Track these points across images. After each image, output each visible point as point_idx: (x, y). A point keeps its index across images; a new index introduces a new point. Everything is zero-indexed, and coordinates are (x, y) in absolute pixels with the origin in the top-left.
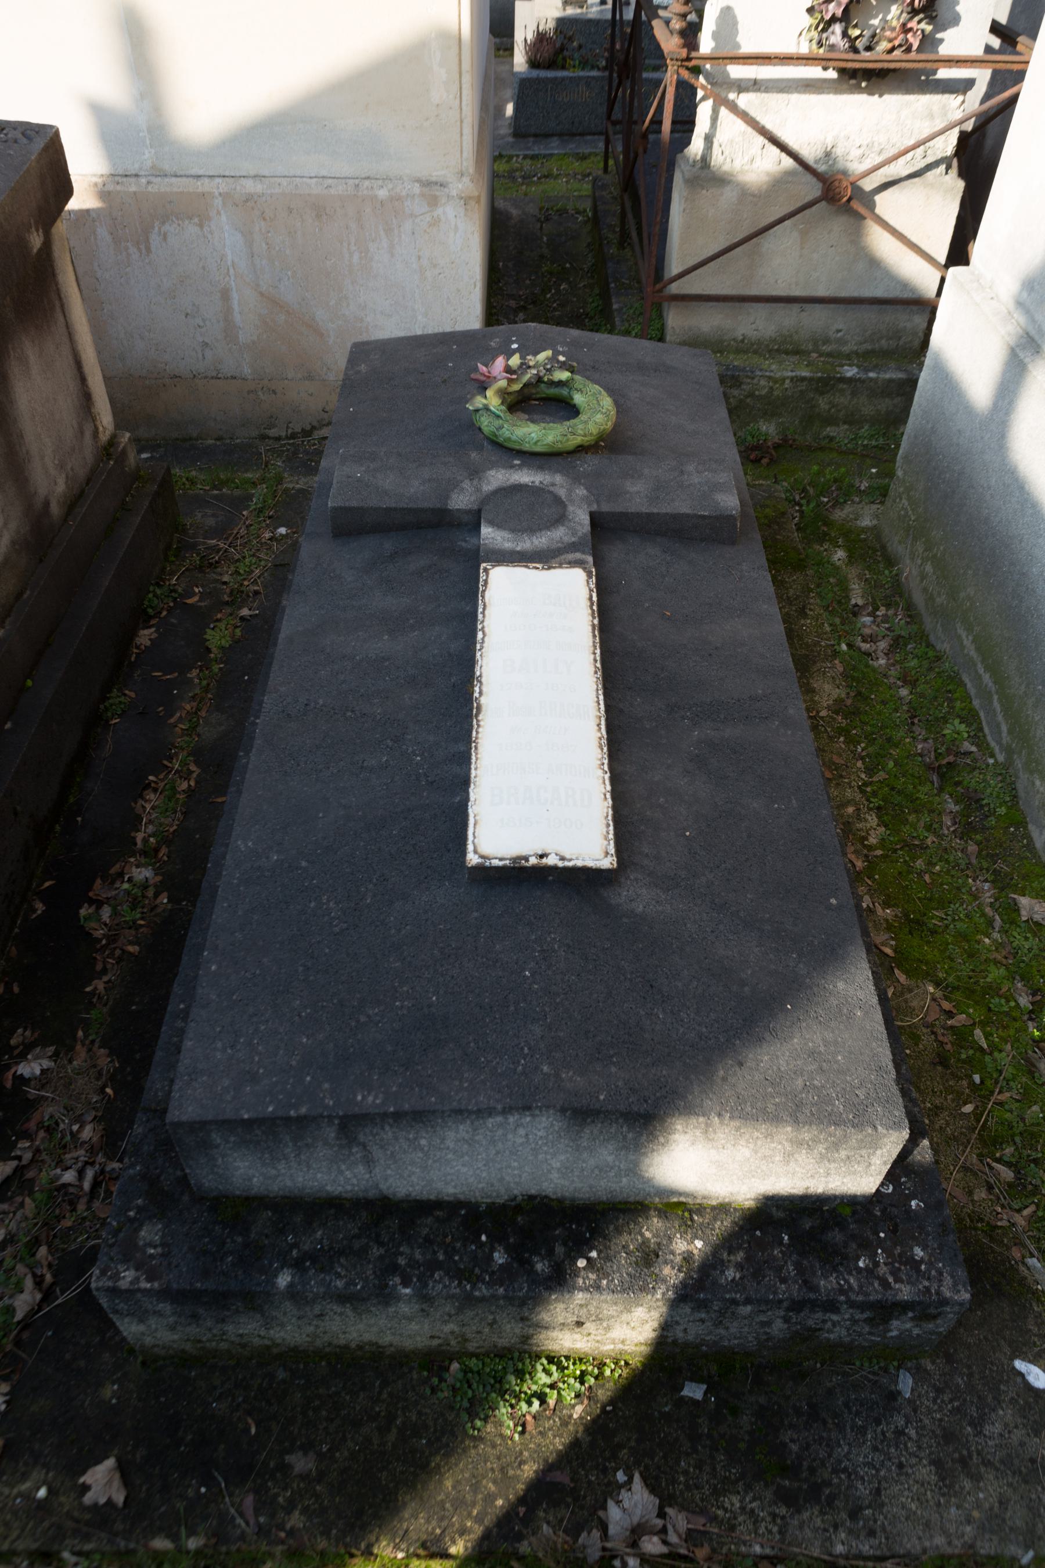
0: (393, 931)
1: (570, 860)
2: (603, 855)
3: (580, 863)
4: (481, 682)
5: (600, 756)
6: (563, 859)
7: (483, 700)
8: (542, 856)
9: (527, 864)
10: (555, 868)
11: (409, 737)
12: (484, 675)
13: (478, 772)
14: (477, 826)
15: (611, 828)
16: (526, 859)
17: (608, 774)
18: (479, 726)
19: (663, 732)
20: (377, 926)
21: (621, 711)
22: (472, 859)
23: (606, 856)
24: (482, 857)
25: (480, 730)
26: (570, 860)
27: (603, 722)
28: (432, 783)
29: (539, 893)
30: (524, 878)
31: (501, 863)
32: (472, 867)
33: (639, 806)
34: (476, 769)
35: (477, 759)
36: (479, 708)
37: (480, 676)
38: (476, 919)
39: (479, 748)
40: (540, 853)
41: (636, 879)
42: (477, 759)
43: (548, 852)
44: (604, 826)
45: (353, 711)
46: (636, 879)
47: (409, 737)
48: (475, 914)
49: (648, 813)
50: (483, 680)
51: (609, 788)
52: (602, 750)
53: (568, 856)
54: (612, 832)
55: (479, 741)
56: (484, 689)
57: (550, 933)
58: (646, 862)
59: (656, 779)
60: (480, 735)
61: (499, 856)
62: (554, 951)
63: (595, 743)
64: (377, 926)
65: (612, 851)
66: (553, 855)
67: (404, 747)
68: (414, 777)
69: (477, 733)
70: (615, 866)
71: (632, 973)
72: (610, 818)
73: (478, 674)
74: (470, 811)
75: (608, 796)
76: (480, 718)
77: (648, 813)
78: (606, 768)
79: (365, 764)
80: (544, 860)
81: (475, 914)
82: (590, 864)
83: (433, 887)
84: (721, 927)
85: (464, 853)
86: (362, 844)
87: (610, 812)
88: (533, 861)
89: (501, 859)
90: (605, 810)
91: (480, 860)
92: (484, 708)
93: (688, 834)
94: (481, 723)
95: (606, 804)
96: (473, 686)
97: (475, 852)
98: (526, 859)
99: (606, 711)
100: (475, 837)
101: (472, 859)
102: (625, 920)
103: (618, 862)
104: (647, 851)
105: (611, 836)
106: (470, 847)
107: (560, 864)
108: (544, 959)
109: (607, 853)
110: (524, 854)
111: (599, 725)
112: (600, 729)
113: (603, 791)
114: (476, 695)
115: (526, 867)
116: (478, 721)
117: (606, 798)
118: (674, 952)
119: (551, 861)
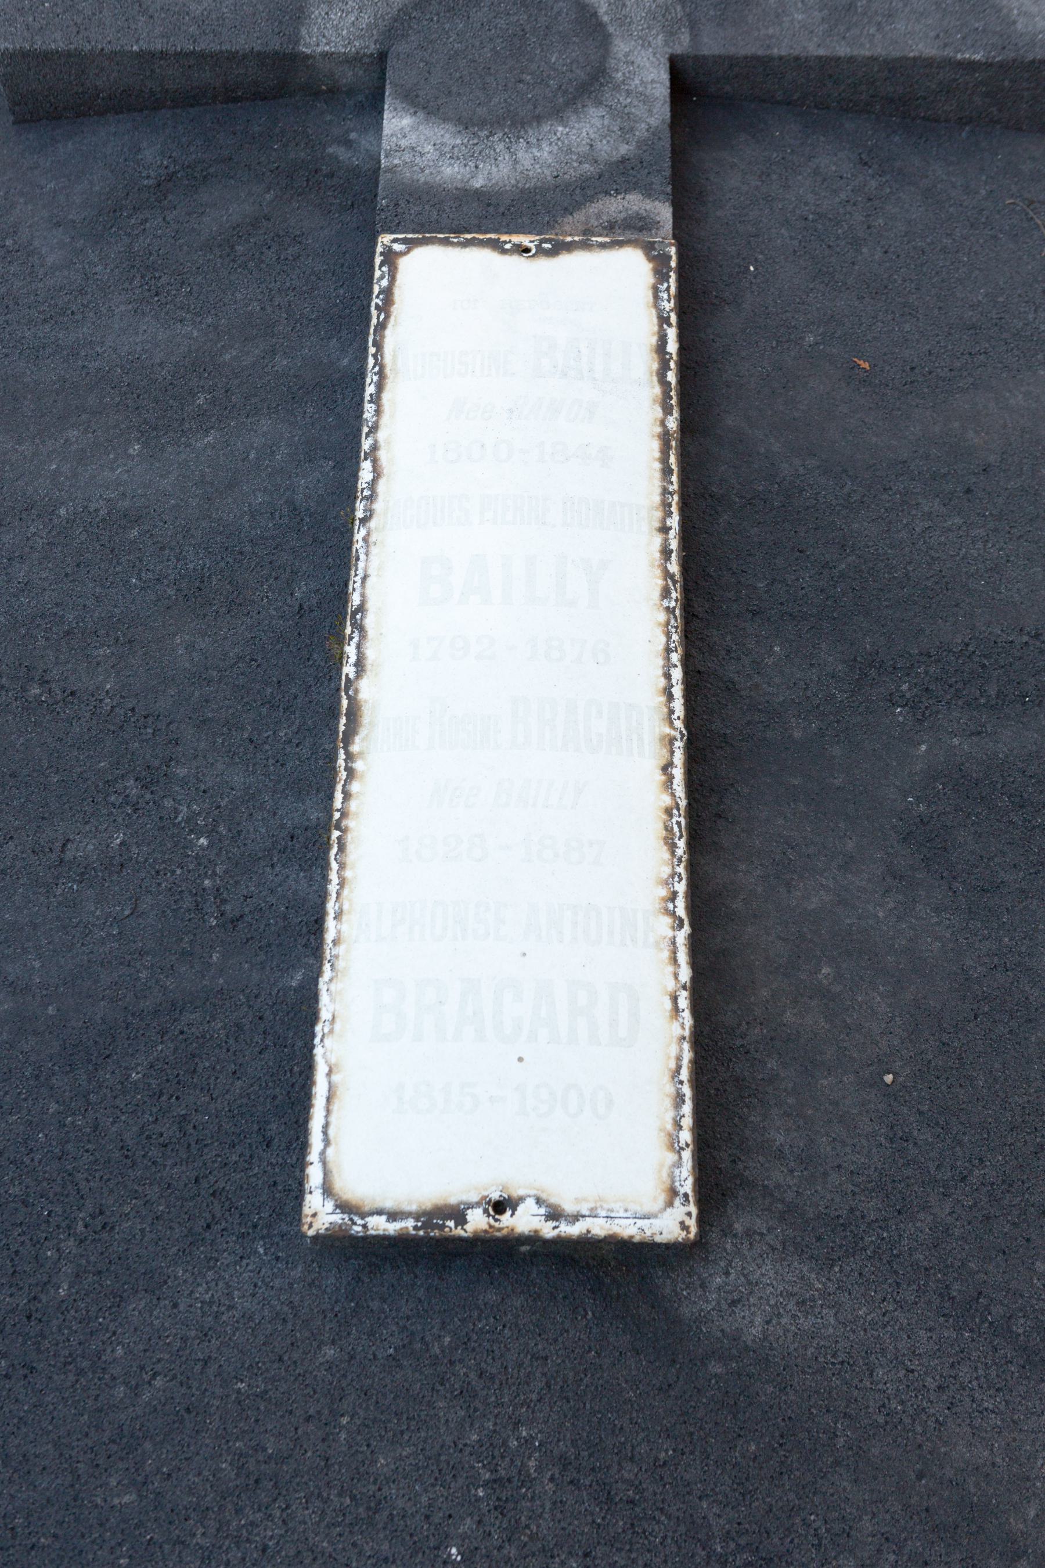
0: (120, 1391)
1: (576, 1218)
2: (662, 1198)
3: (599, 1228)
4: (360, 628)
5: (667, 871)
6: (554, 1215)
7: (367, 690)
8: (500, 1207)
9: (459, 1232)
10: (534, 1239)
11: (181, 772)
12: (370, 605)
13: (344, 927)
14: (335, 1107)
15: (687, 1108)
16: (459, 1215)
17: (687, 929)
18: (351, 772)
19: (837, 751)
20: (80, 1372)
21: (731, 688)
22: (319, 1213)
23: (670, 1204)
24: (344, 1207)
25: (355, 787)
26: (576, 1218)
27: (679, 758)
28: (235, 921)
29: (492, 1296)
30: (456, 1266)
31: (392, 1228)
32: (316, 1238)
33: (765, 993)
34: (338, 916)
35: (342, 884)
36: (354, 714)
37: (361, 609)
38: (330, 1366)
39: (350, 847)
40: (495, 1196)
41: (749, 1233)
42: (342, 884)
43: (517, 1192)
44: (668, 1103)
45: (44, 682)
46: (749, 1233)
47: (181, 772)
48: (330, 1352)
49: (789, 1016)
50: (370, 622)
51: (685, 974)
52: (672, 847)
53: (569, 1208)
54: (687, 1122)
55: (350, 823)
56: (370, 653)
57: (517, 1424)
58: (777, 1176)
59: (813, 904)
60: (353, 805)
61: (389, 1204)
62: (526, 1481)
63: (652, 827)
64: (80, 1372)
65: (687, 1187)
66: (530, 1202)
67: (168, 803)
68: (188, 903)
69: (347, 796)
70: (694, 1230)
71: (727, 1536)
72: (685, 1075)
73: (356, 599)
74: (318, 1051)
75: (684, 1002)
76: (355, 748)
77: (789, 1016)
78: (681, 911)
79: (69, 855)
80: (506, 1220)
81: (330, 1352)
82: (628, 1229)
83: (226, 1258)
84: (964, 1372)
85: (297, 1192)
86: (53, 1107)
87: (687, 1056)
88: (477, 1221)
89: (393, 1216)
90: (674, 1050)
91: (337, 1218)
92: (367, 717)
93: (889, 1078)
94: (358, 765)
95: (676, 1030)
96: (341, 640)
97: (327, 1190)
98: (459, 1215)
99: (688, 721)
100: (327, 1142)
101: (319, 1213)
102: (716, 1368)
103: (701, 1221)
104: (780, 1139)
105: (686, 1136)
106: (314, 1175)
107: (548, 1230)
108: (500, 1509)
109: (673, 1192)
110: (453, 1200)
111: (667, 768)
112: (671, 778)
113: (671, 985)
114: (349, 670)
115: (461, 1239)
116: (350, 757)
117: (676, 1010)
118: (837, 1463)
119: (525, 1220)
